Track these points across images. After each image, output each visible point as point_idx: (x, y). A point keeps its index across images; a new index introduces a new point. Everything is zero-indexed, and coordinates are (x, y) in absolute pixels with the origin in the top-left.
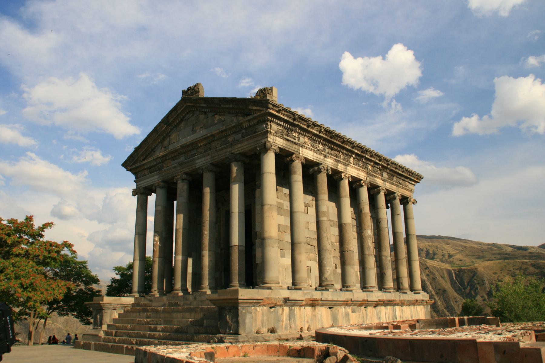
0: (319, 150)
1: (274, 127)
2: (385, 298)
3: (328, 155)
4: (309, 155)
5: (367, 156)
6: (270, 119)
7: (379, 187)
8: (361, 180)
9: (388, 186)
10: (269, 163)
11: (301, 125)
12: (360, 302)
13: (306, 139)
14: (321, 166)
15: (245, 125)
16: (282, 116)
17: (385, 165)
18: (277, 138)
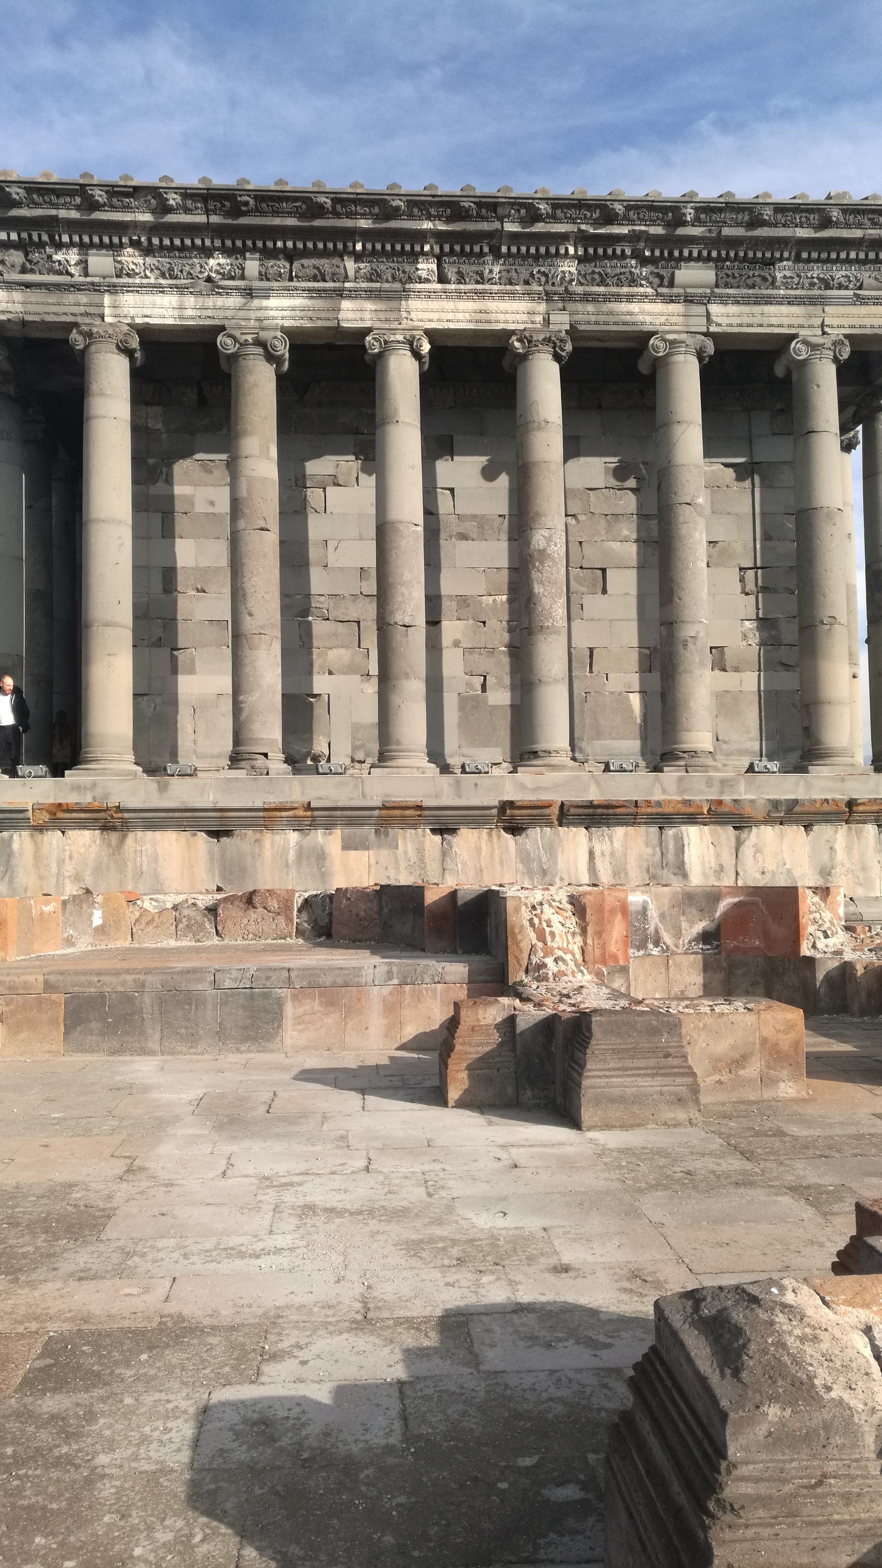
2: (594, 795)
4: (157, 312)
5: (511, 227)
8: (513, 332)
9: (728, 317)
11: (63, 213)
12: (376, 813)
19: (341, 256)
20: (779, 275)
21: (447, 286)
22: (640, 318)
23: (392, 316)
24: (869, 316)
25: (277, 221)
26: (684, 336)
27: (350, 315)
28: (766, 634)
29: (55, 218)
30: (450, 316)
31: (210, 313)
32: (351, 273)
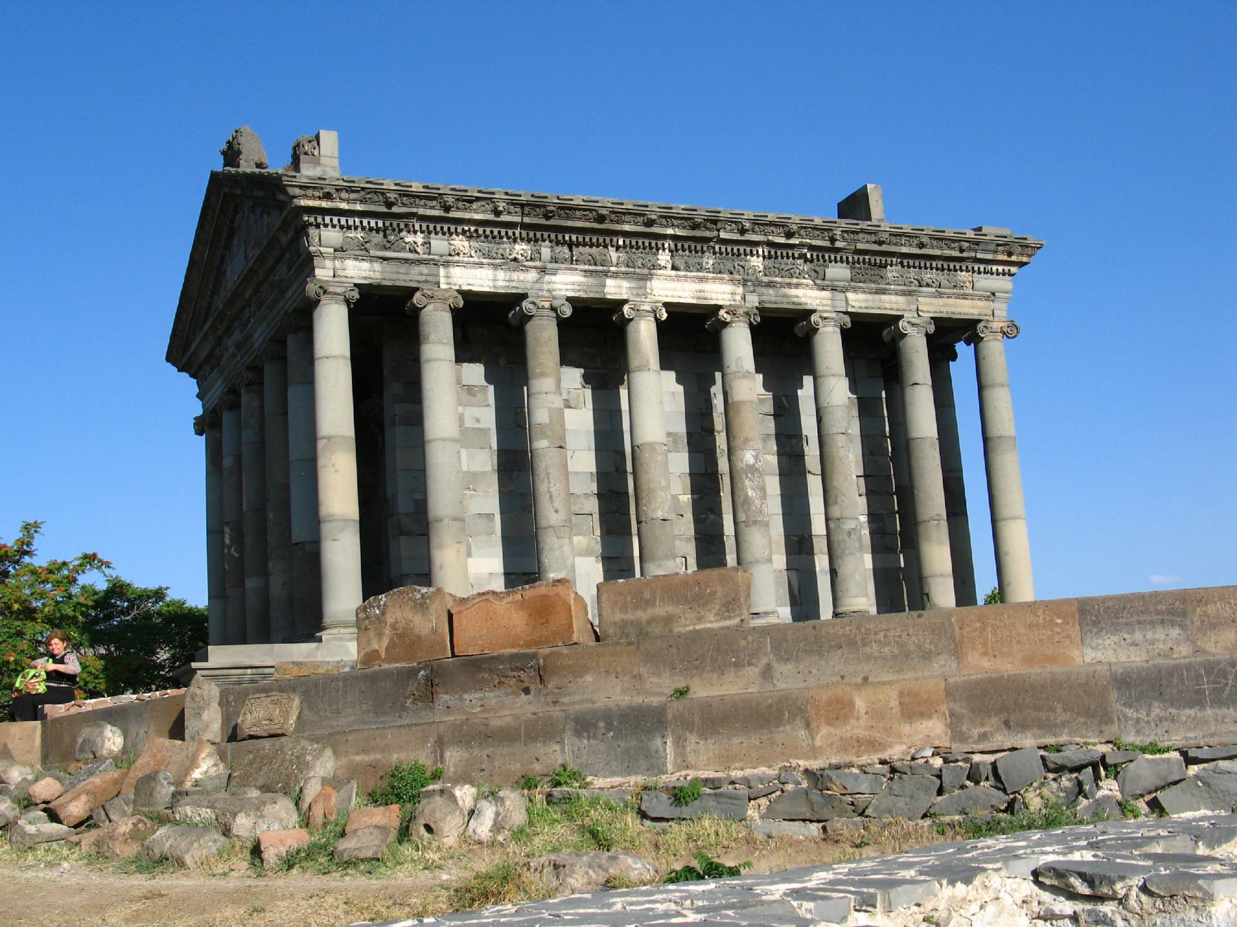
0: (515, 260)
1: (327, 237)
3: (550, 266)
4: (477, 282)
5: (723, 235)
6: (312, 220)
7: (813, 311)
8: (721, 307)
9: (859, 301)
10: (333, 332)
11: (421, 211)
13: (460, 243)
14: (525, 304)
15: (284, 239)
16: (344, 206)
17: (814, 242)
18: (350, 263)
19: (606, 246)
20: (890, 275)
21: (679, 273)
22: (803, 300)
23: (641, 292)
24: (944, 305)
25: (570, 223)
26: (834, 315)
27: (612, 290)
28: (875, 526)
29: (414, 215)
30: (680, 294)
31: (514, 284)
32: (614, 261)
